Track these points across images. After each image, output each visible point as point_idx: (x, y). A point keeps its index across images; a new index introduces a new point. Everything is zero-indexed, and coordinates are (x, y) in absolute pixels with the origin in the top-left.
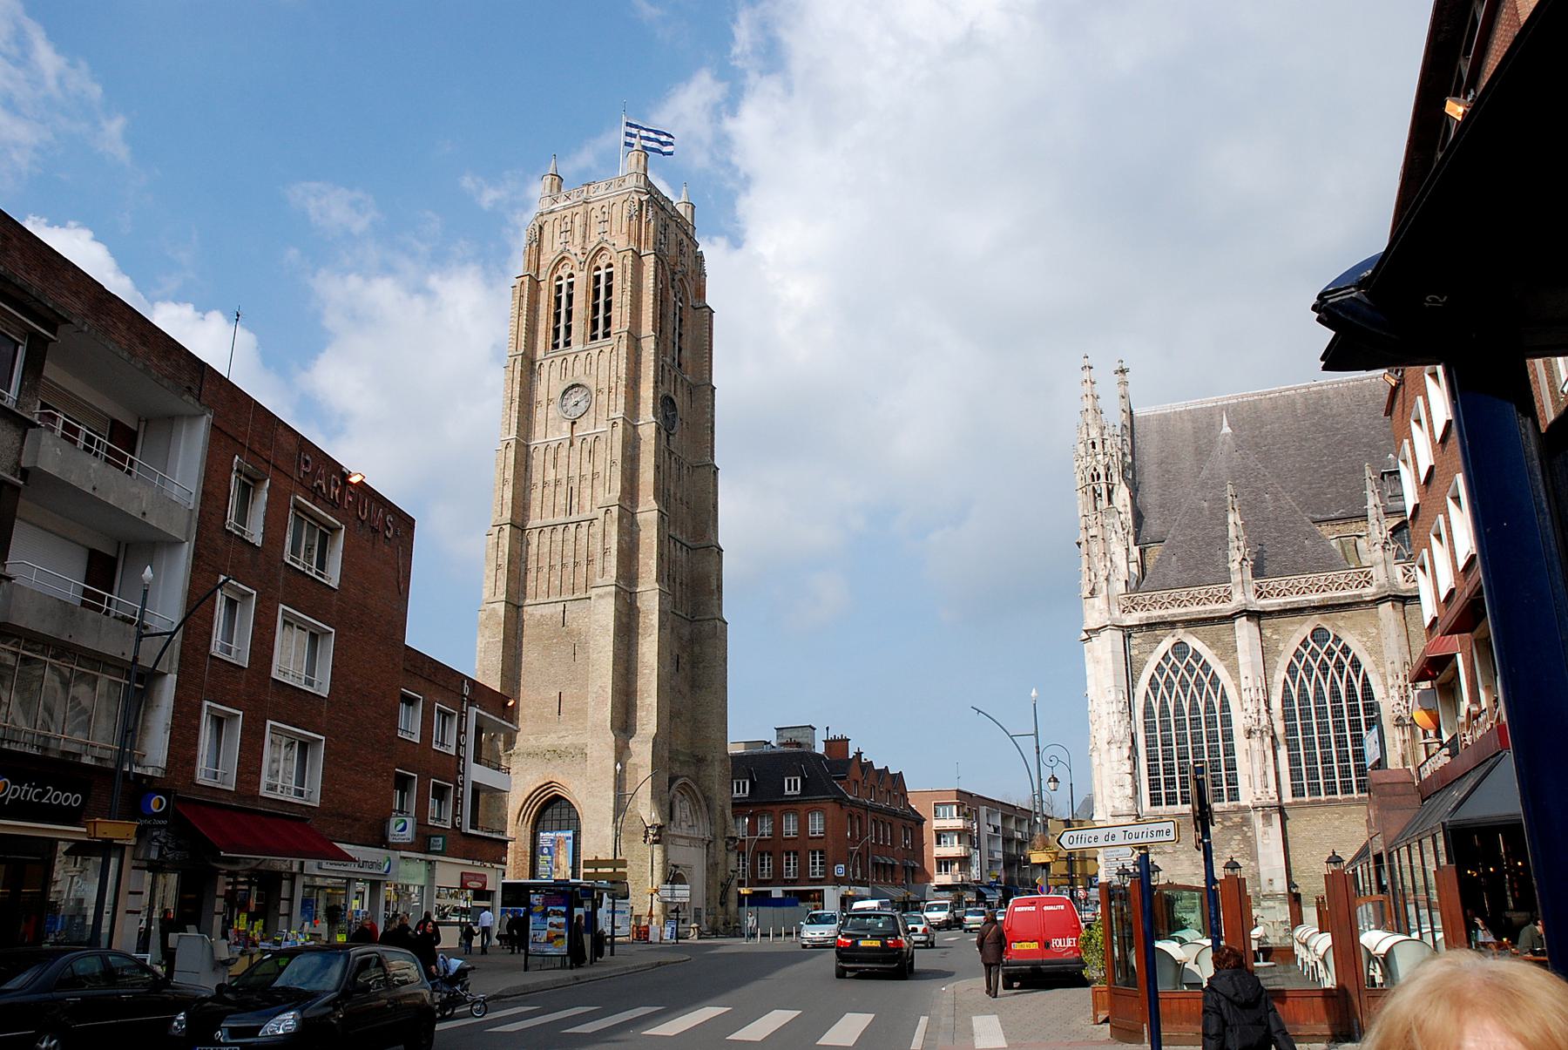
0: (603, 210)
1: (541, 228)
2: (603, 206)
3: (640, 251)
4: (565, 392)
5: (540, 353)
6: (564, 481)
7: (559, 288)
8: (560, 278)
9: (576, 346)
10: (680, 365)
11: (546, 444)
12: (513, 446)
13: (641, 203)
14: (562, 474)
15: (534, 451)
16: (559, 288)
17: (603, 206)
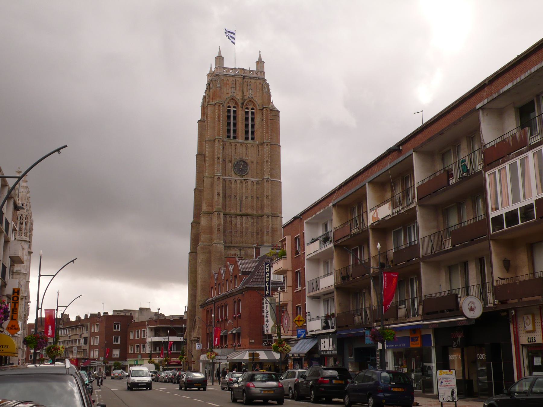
10: (253, 139)
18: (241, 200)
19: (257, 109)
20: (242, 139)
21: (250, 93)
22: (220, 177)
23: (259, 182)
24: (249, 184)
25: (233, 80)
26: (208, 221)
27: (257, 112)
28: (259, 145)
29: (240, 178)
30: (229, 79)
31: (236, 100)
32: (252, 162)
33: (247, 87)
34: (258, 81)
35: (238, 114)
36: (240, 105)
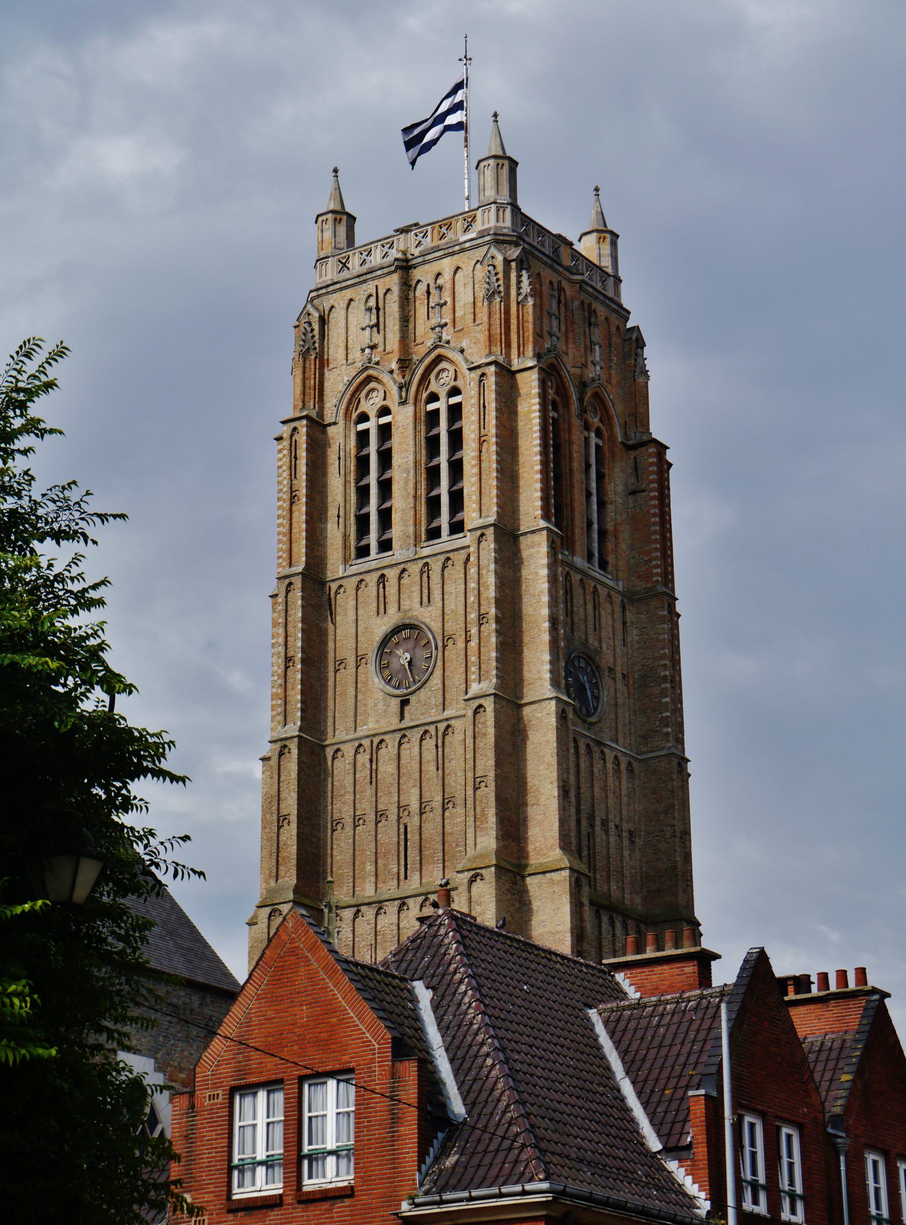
0: (440, 281)
1: (323, 321)
2: (439, 274)
3: (510, 362)
4: (385, 641)
5: (335, 567)
6: (393, 817)
7: (363, 437)
8: (364, 418)
9: (399, 553)
10: (603, 565)
11: (357, 743)
12: (295, 751)
13: (507, 262)
14: (388, 803)
15: (334, 758)
16: (363, 437)
17: (439, 274)
18: (589, 834)
19: (612, 437)
20: (583, 558)
21: (598, 359)
22: (567, 709)
23: (635, 764)
24: (610, 765)
25: (551, 282)
26: (512, 910)
27: (613, 454)
28: (625, 600)
29: (584, 729)
30: (542, 274)
31: (564, 373)
32: (611, 670)
33: (587, 332)
34: (614, 318)
35: (570, 442)
36: (575, 406)
